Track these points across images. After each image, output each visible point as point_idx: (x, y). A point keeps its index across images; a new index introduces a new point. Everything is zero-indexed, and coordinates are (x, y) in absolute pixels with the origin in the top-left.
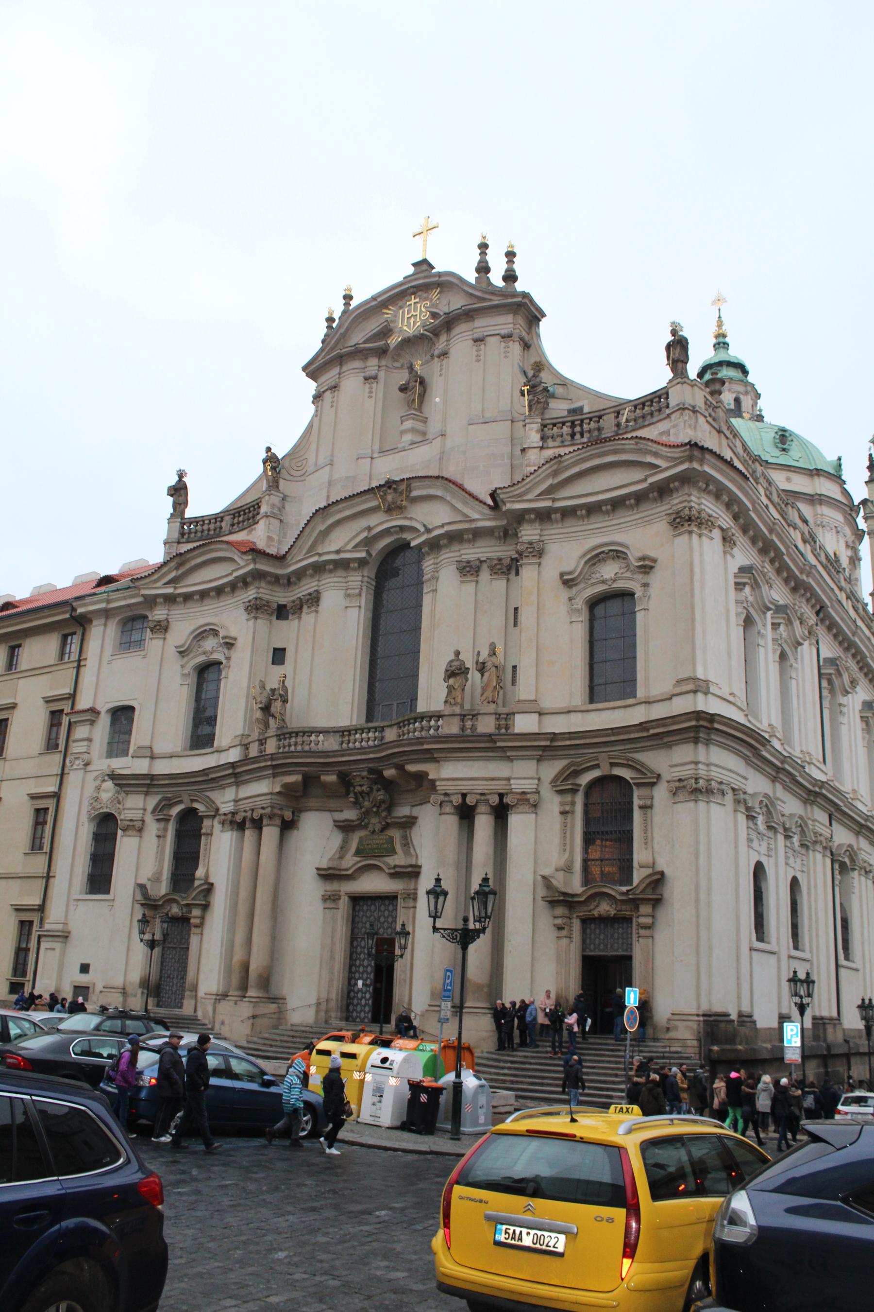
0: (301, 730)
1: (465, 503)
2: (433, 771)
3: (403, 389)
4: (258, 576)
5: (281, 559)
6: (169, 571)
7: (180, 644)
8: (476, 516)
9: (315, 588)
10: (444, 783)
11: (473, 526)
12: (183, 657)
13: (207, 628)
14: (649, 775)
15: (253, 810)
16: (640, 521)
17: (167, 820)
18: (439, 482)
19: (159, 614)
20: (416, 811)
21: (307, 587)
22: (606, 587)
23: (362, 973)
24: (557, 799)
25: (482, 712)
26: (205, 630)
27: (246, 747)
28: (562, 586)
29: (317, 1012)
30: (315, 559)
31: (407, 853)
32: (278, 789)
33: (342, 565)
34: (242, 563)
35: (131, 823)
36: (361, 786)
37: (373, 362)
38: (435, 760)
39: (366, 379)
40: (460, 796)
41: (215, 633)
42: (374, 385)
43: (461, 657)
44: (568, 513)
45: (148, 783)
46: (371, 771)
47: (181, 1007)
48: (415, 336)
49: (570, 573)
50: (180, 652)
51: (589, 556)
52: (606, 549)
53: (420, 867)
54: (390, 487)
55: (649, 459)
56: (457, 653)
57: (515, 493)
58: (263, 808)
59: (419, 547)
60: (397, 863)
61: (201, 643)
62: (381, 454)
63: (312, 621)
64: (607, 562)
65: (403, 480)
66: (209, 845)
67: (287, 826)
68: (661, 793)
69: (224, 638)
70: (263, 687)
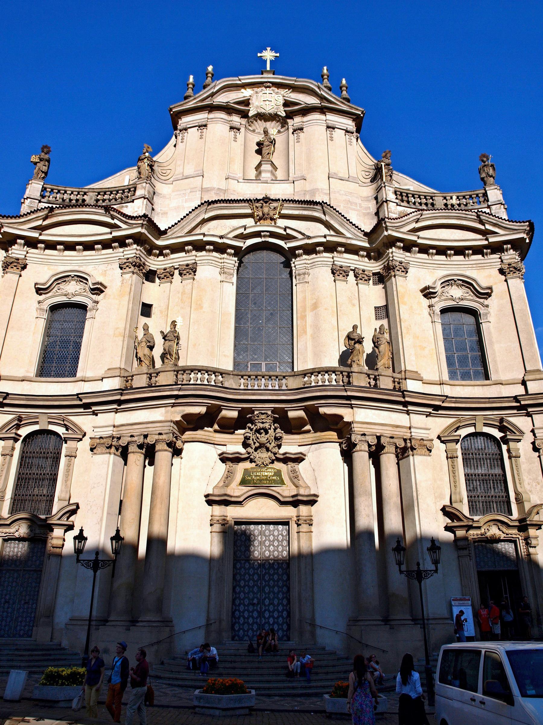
0: (204, 368)
1: (342, 225)
2: (347, 414)
3: (259, 144)
4: (138, 239)
5: (161, 233)
6: (36, 219)
7: (42, 281)
8: (348, 235)
9: (194, 261)
10: (359, 425)
11: (349, 241)
12: (41, 294)
13: (73, 274)
14: (518, 434)
15: (146, 436)
16: (474, 266)
17: (16, 440)
18: (319, 207)
19: (18, 251)
20: (302, 449)
21: (179, 259)
23: (248, 593)
24: (443, 446)
25: (383, 374)
26: (70, 276)
27: (128, 378)
28: (423, 297)
29: (208, 633)
30: (201, 237)
32: (178, 418)
33: (221, 248)
34: (123, 226)
36: (263, 423)
37: (236, 119)
38: (351, 406)
39: (232, 128)
40: (375, 437)
41: (82, 279)
42: (238, 134)
43: (359, 331)
44: (424, 249)
47: (30, 636)
48: (270, 114)
49: (434, 288)
51: (443, 280)
52: (455, 278)
53: (317, 496)
54: (266, 202)
55: (488, 227)
56: (355, 327)
57: (396, 225)
58: (160, 434)
59: (293, 250)
60: (286, 493)
61: (61, 286)
62: (246, 181)
63: (190, 286)
64: (453, 287)
65: (279, 200)
66: (69, 466)
67: (177, 452)
69: (94, 284)
70: (146, 328)
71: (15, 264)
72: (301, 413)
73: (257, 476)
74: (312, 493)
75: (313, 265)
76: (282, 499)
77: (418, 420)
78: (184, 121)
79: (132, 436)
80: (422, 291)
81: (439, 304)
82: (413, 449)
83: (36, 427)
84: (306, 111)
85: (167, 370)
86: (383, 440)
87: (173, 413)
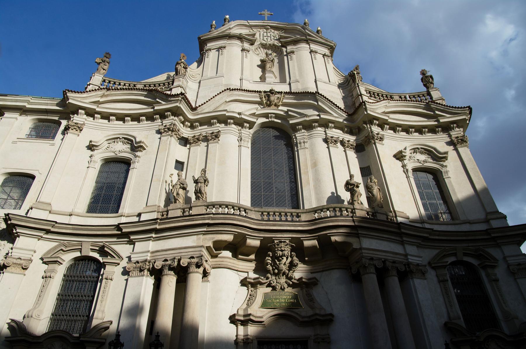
6: (96, 96)
13: (121, 136)
22: (421, 165)
31: (312, 308)
33: (240, 122)
34: (164, 103)
35: (19, 261)
37: (246, 45)
39: (243, 50)
44: (394, 128)
45: (47, 229)
46: (290, 241)
50: (94, 146)
52: (419, 147)
54: (272, 93)
60: (303, 314)
65: (281, 92)
68: (500, 272)
71: (75, 127)
72: (315, 242)
73: (277, 299)
74: (328, 312)
75: (310, 137)
76: (301, 319)
77: (411, 250)
78: (210, 45)
79: (166, 260)
80: (395, 156)
81: (410, 166)
82: (411, 272)
83: (78, 254)
84: (295, 42)
85: (198, 205)
86: (388, 263)
87: (205, 239)
